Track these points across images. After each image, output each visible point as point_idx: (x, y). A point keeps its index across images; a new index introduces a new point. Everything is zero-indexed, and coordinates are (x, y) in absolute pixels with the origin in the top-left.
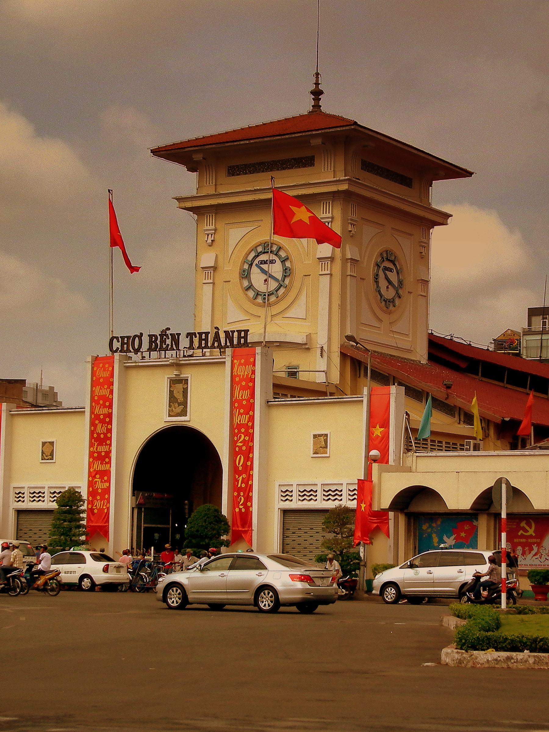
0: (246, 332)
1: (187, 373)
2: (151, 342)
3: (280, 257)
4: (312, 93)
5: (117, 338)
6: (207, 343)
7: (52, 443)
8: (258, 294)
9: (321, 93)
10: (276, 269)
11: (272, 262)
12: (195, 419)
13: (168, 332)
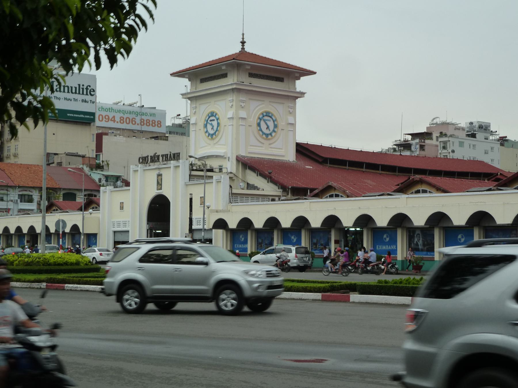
0: (179, 153)
4: (241, 42)
9: (245, 42)
10: (215, 123)
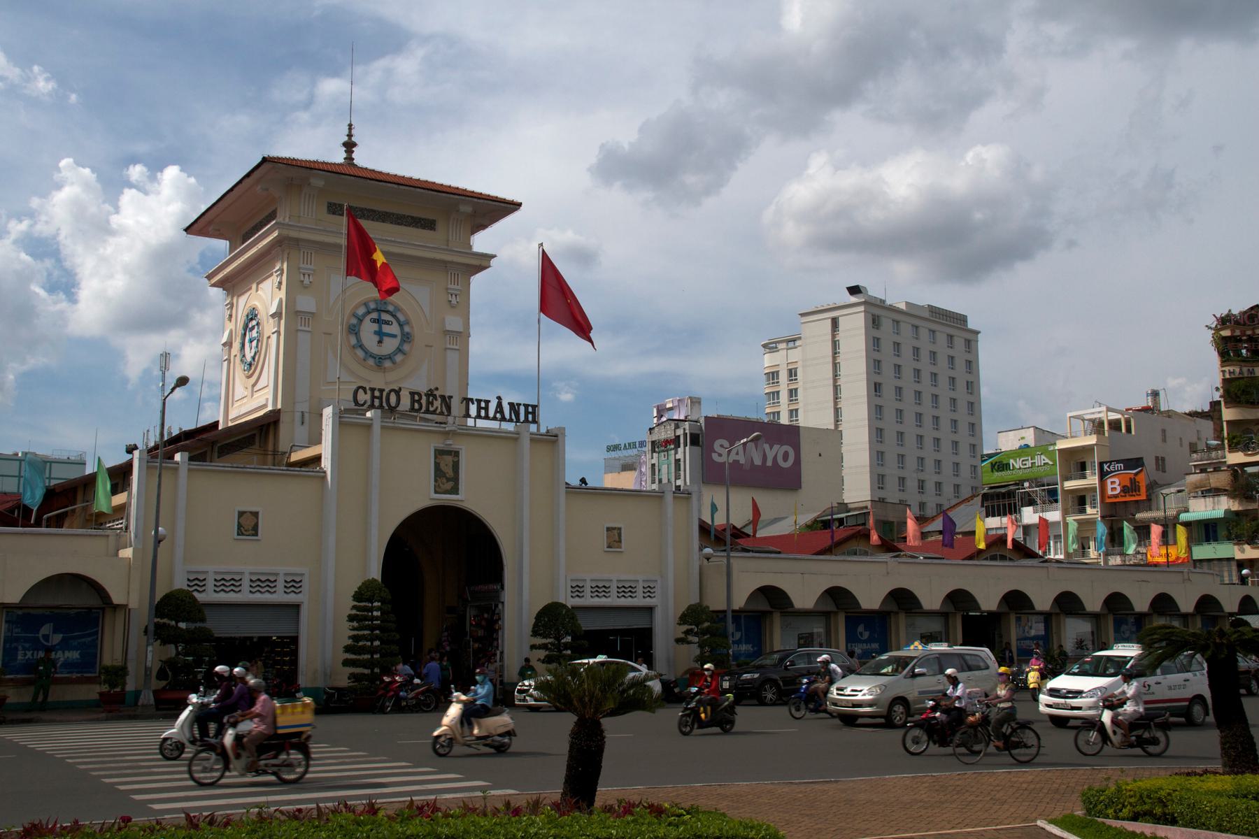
2: (413, 401)
4: (345, 144)
5: (364, 389)
6: (487, 413)
7: (256, 514)
8: (373, 356)
9: (354, 145)
11: (387, 323)
12: (469, 498)
13: (437, 393)
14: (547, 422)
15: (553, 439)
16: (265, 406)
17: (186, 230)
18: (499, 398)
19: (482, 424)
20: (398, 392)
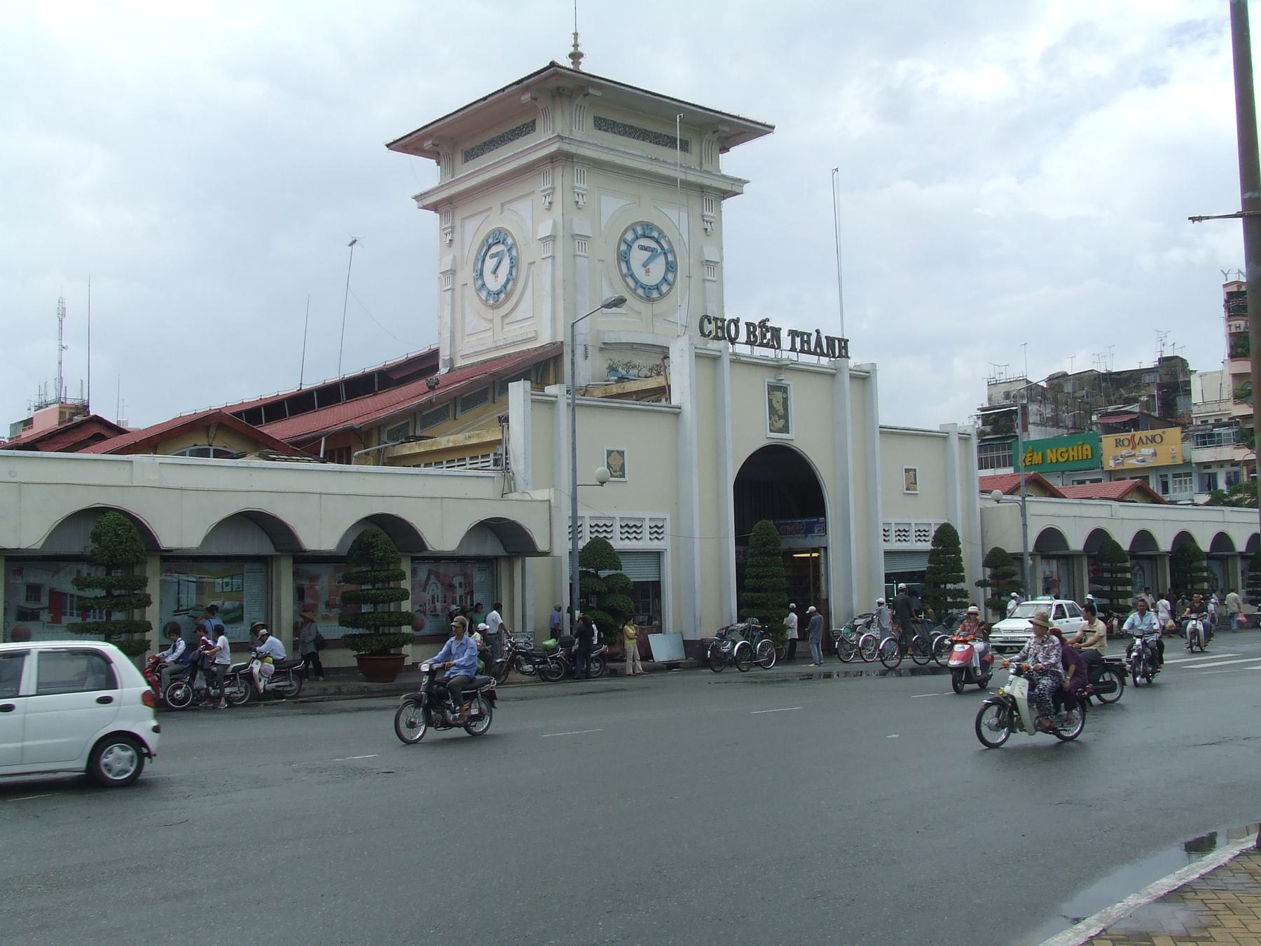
1: (787, 379)
3: (662, 248)
7: (621, 453)
9: (581, 55)
14: (856, 359)
15: (863, 378)
16: (535, 339)
17: (388, 146)
18: (818, 331)
19: (805, 358)
20: (736, 322)
